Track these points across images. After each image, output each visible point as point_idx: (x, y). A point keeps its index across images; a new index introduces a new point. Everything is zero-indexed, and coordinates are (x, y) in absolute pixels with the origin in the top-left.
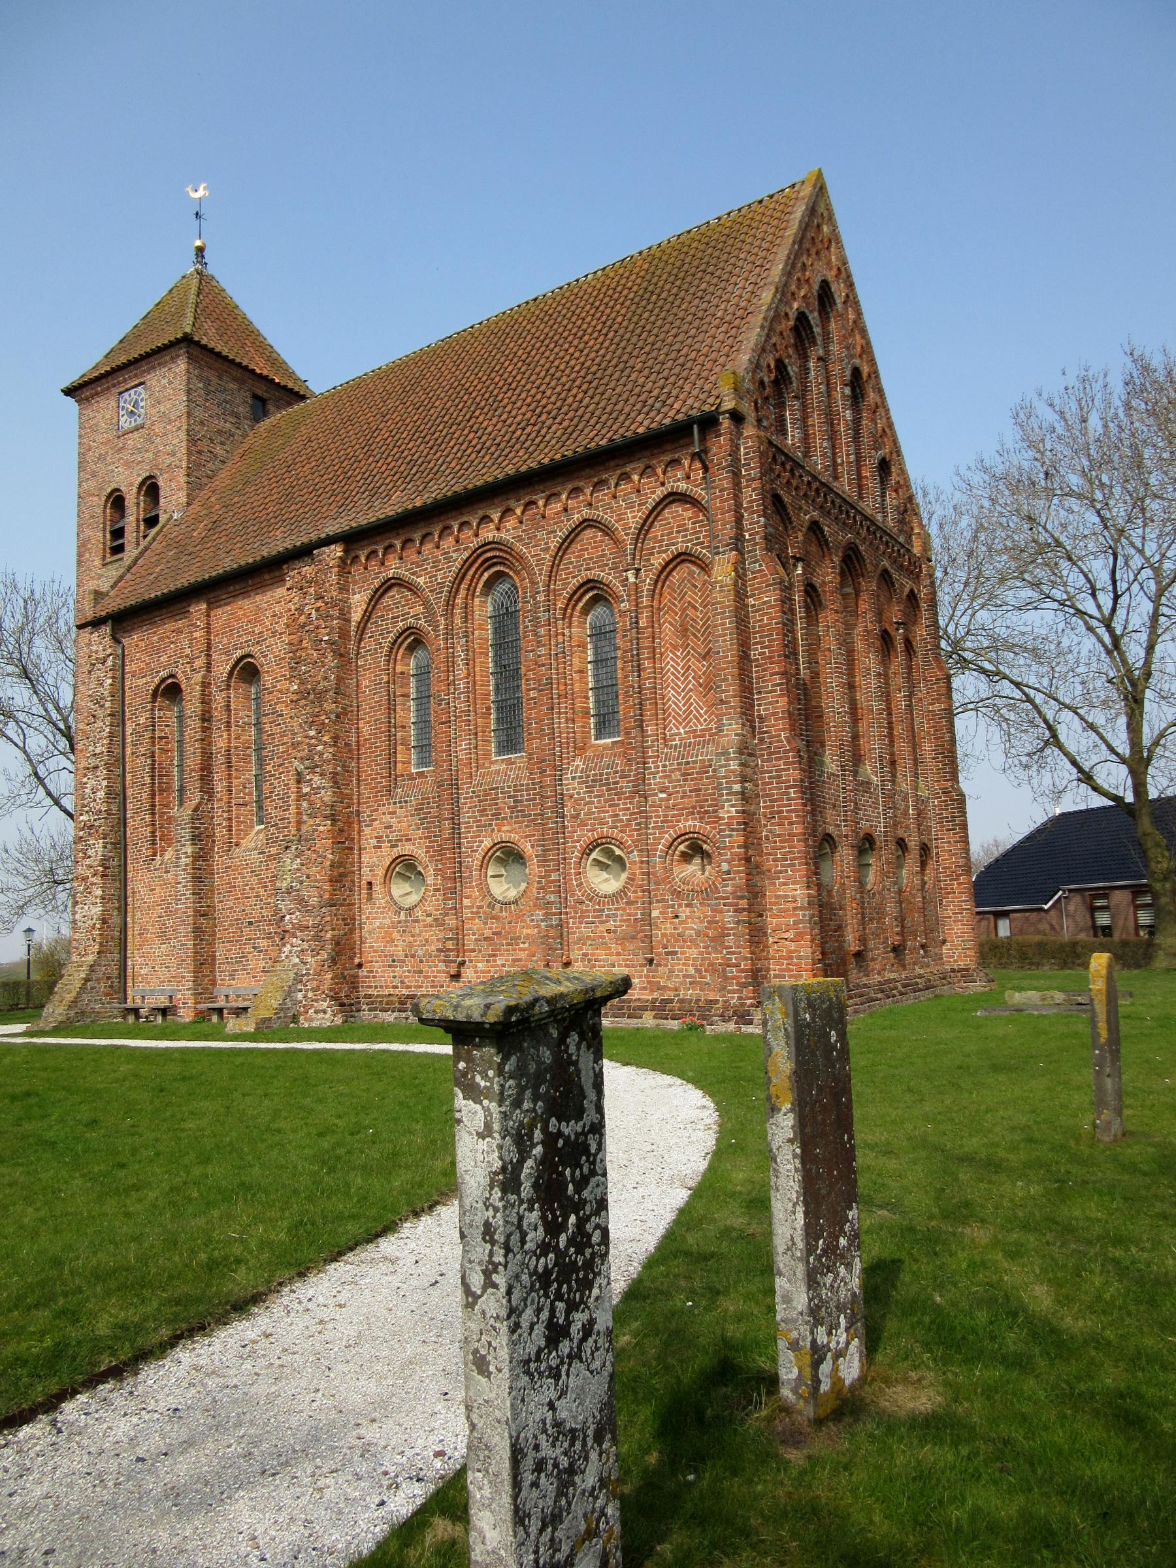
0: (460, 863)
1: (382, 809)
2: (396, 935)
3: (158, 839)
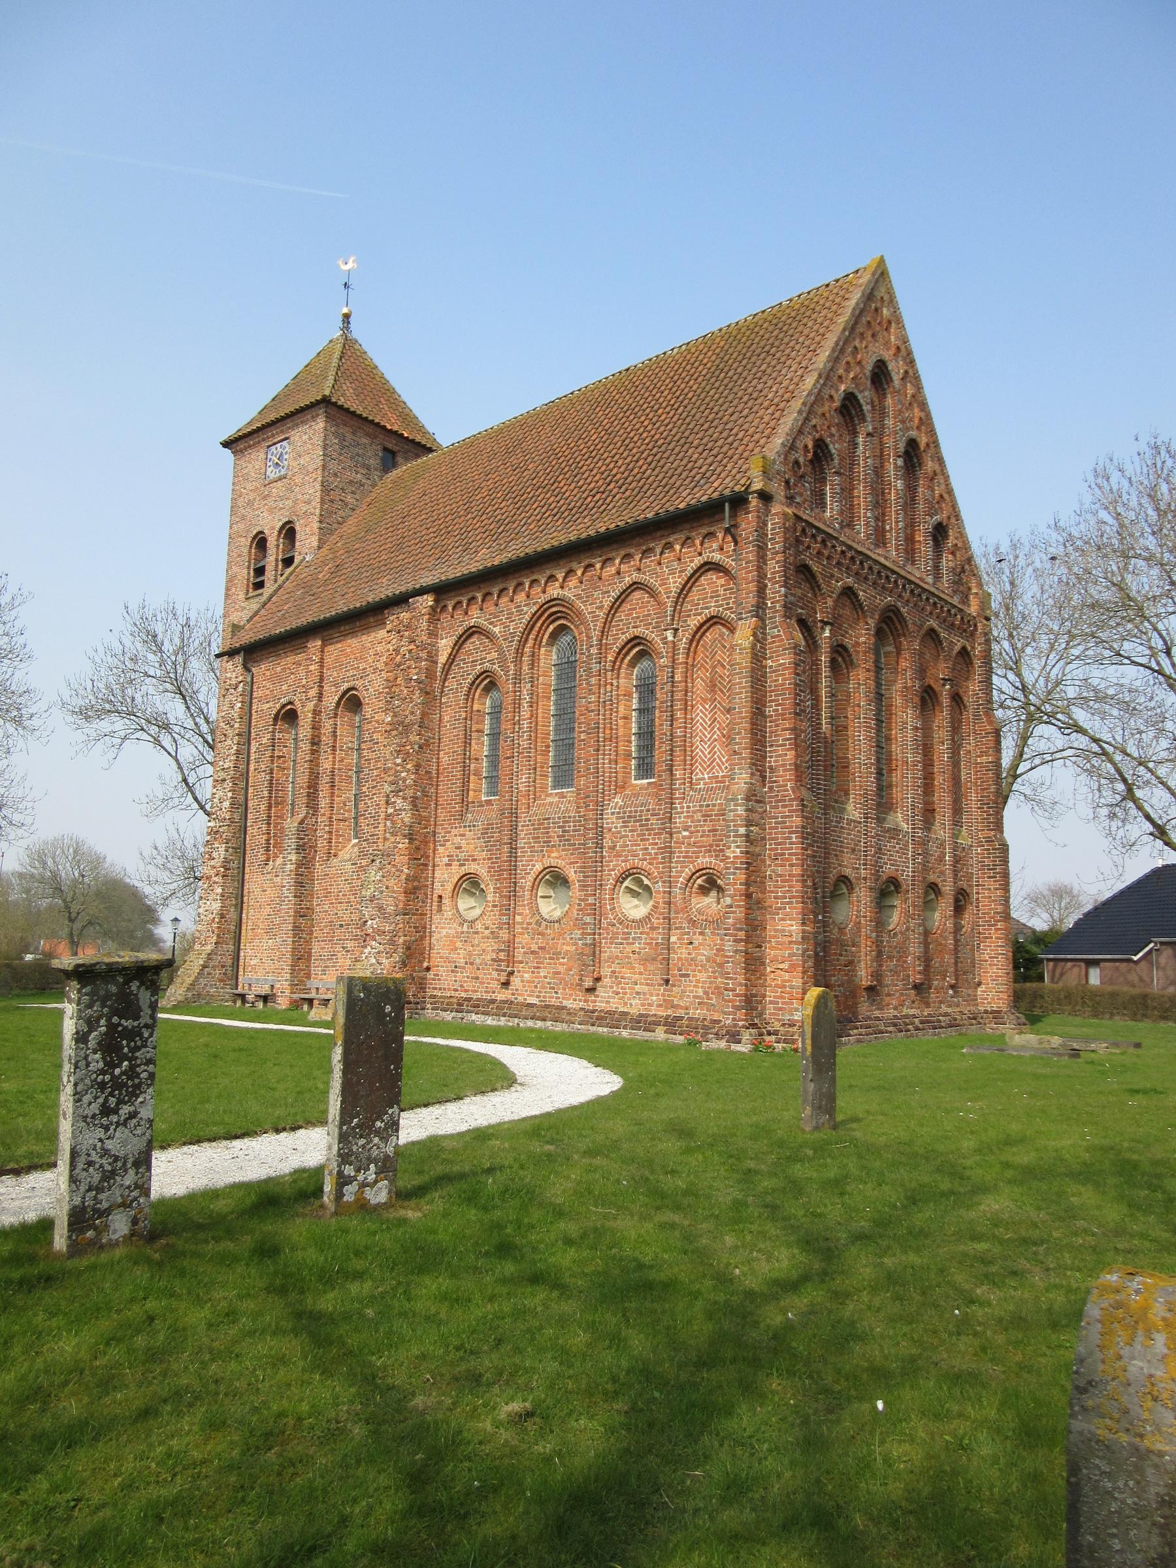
0: (515, 883)
1: (454, 832)
2: (459, 944)
3: (272, 847)
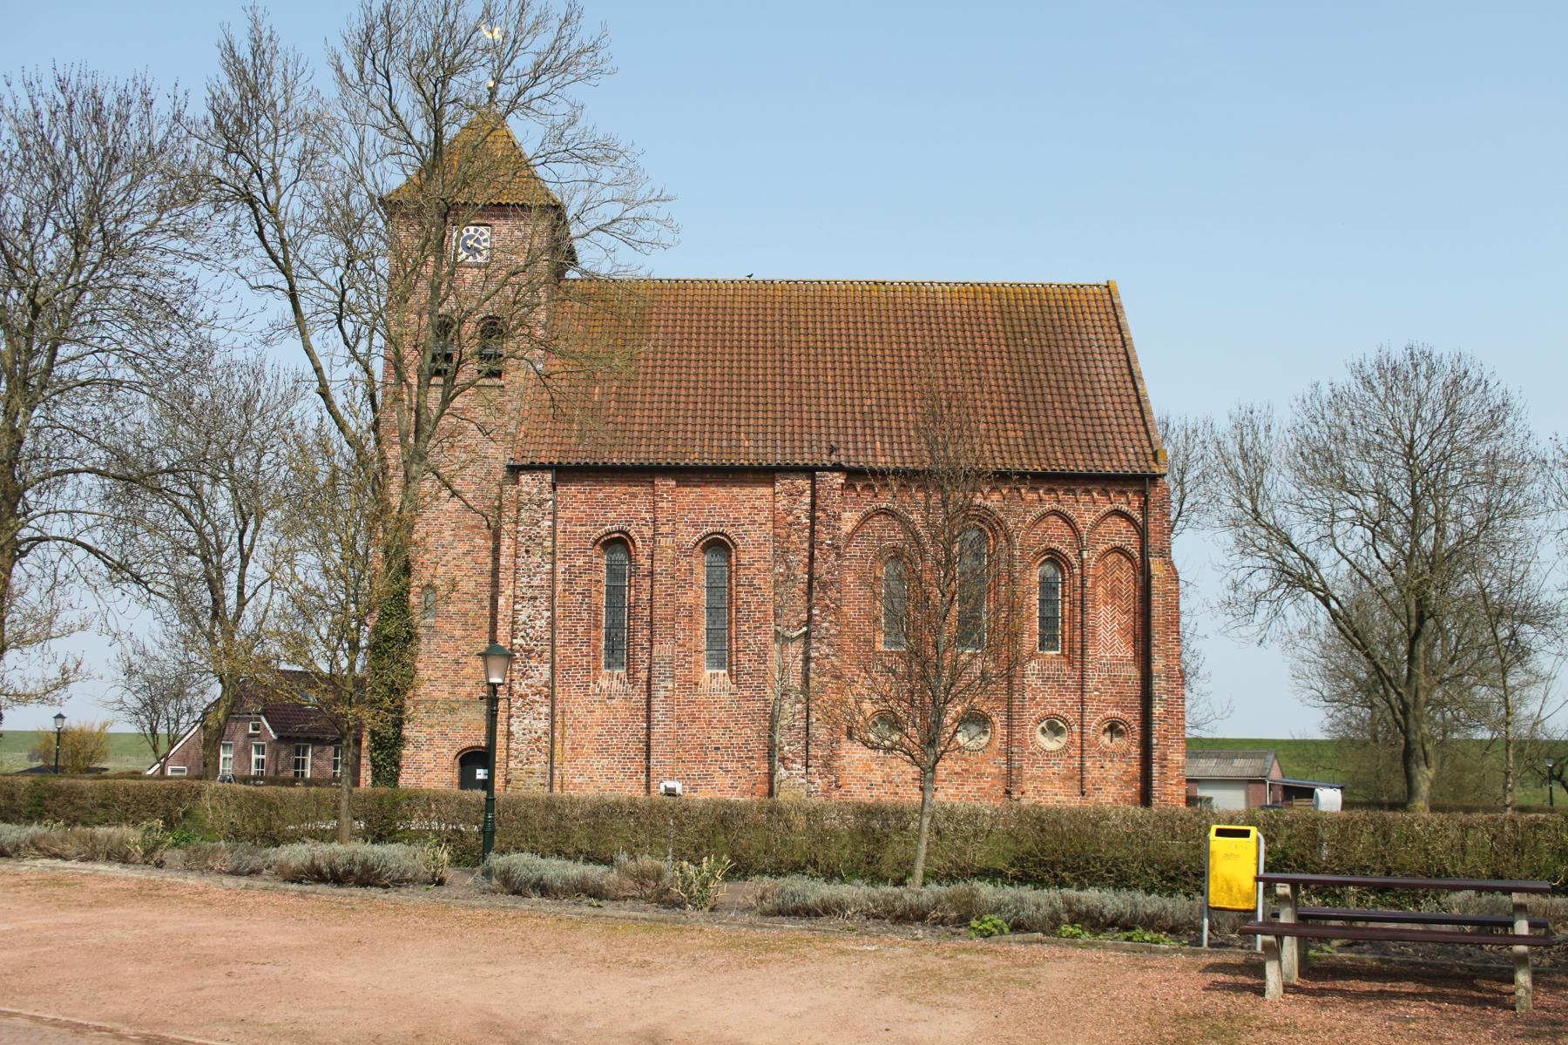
2: (874, 766)
